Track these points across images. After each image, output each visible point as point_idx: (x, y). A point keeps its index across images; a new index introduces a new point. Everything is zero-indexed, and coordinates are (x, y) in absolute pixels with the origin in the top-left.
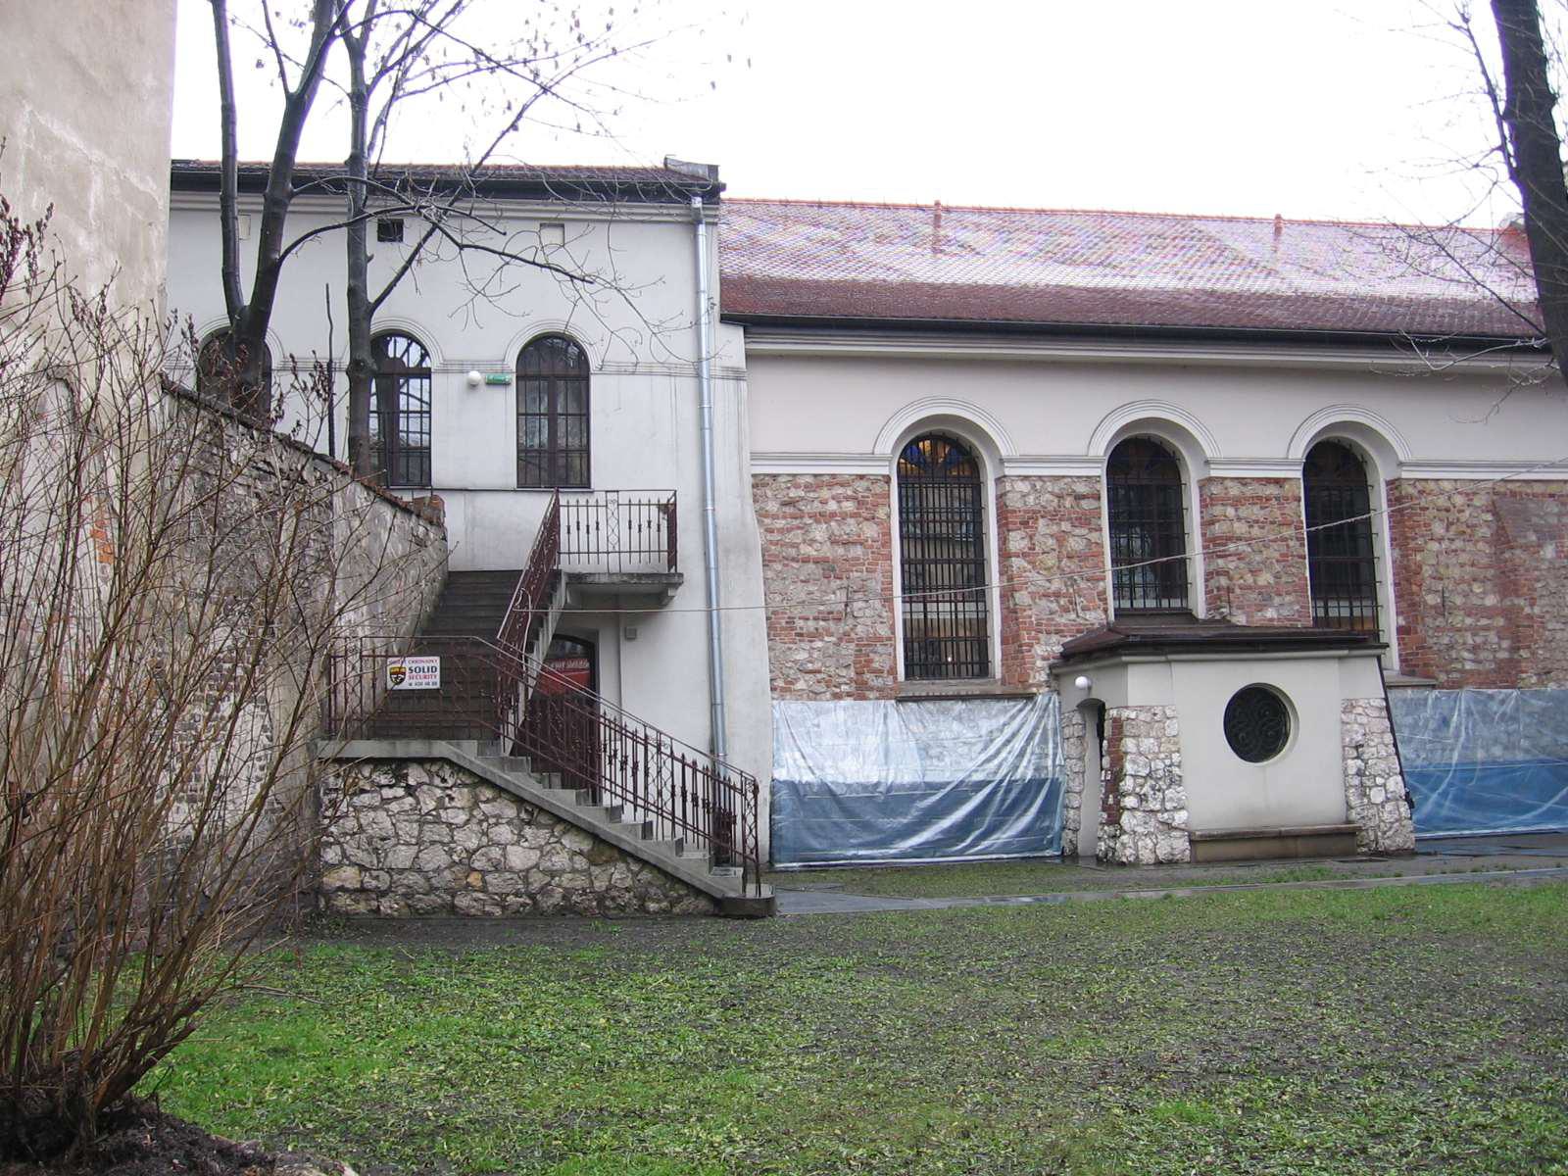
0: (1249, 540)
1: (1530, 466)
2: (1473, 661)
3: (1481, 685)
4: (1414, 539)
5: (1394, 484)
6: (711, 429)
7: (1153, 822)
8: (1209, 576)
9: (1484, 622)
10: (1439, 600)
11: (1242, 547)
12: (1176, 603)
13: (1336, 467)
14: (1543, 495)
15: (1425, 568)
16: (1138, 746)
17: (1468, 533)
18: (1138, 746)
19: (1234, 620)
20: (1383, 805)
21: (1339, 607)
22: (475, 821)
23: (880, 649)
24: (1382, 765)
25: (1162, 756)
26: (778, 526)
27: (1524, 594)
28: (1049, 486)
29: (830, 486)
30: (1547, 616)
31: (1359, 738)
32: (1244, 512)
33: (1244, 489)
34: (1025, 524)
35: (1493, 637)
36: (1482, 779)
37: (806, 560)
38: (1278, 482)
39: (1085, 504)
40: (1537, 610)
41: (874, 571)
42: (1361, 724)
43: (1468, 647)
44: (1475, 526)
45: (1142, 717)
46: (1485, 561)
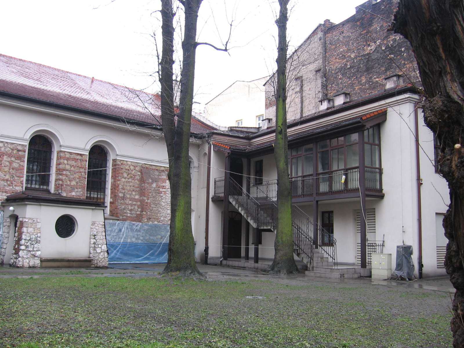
0: (70, 171)
1: (152, 161)
2: (130, 214)
3: (132, 221)
4: (118, 177)
5: (114, 160)
7: (29, 254)
8: (56, 180)
9: (134, 203)
10: (123, 195)
11: (68, 173)
12: (45, 187)
13: (99, 153)
14: (155, 169)
15: (120, 186)
16: (27, 230)
17: (133, 177)
18: (27, 230)
19: (62, 194)
20: (100, 253)
21: (94, 194)
24: (101, 241)
25: (35, 234)
27: (146, 196)
28: (9, 146)
30: (152, 203)
31: (95, 233)
32: (70, 162)
33: (70, 155)
36: (129, 247)
38: (81, 155)
39: (20, 153)
40: (149, 201)
42: (96, 229)
44: (135, 175)
45: (30, 221)
46: (137, 186)
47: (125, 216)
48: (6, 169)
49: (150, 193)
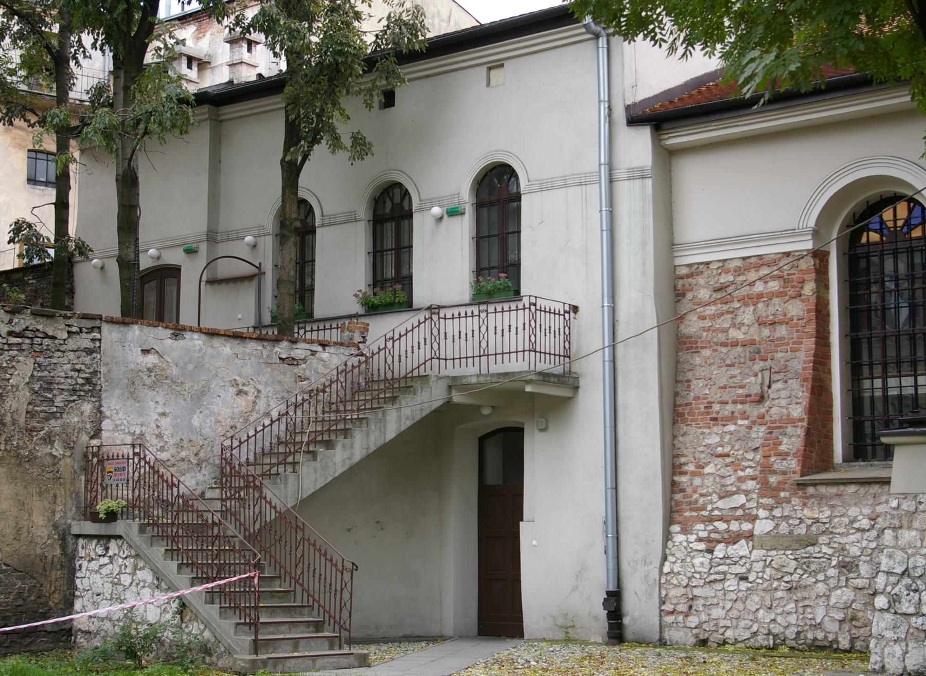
6: (602, 231)
7: (904, 628)
16: (896, 538)
18: (896, 538)
22: (134, 584)
23: (789, 430)
26: (708, 312)
29: (758, 267)
37: (735, 344)
41: (799, 350)
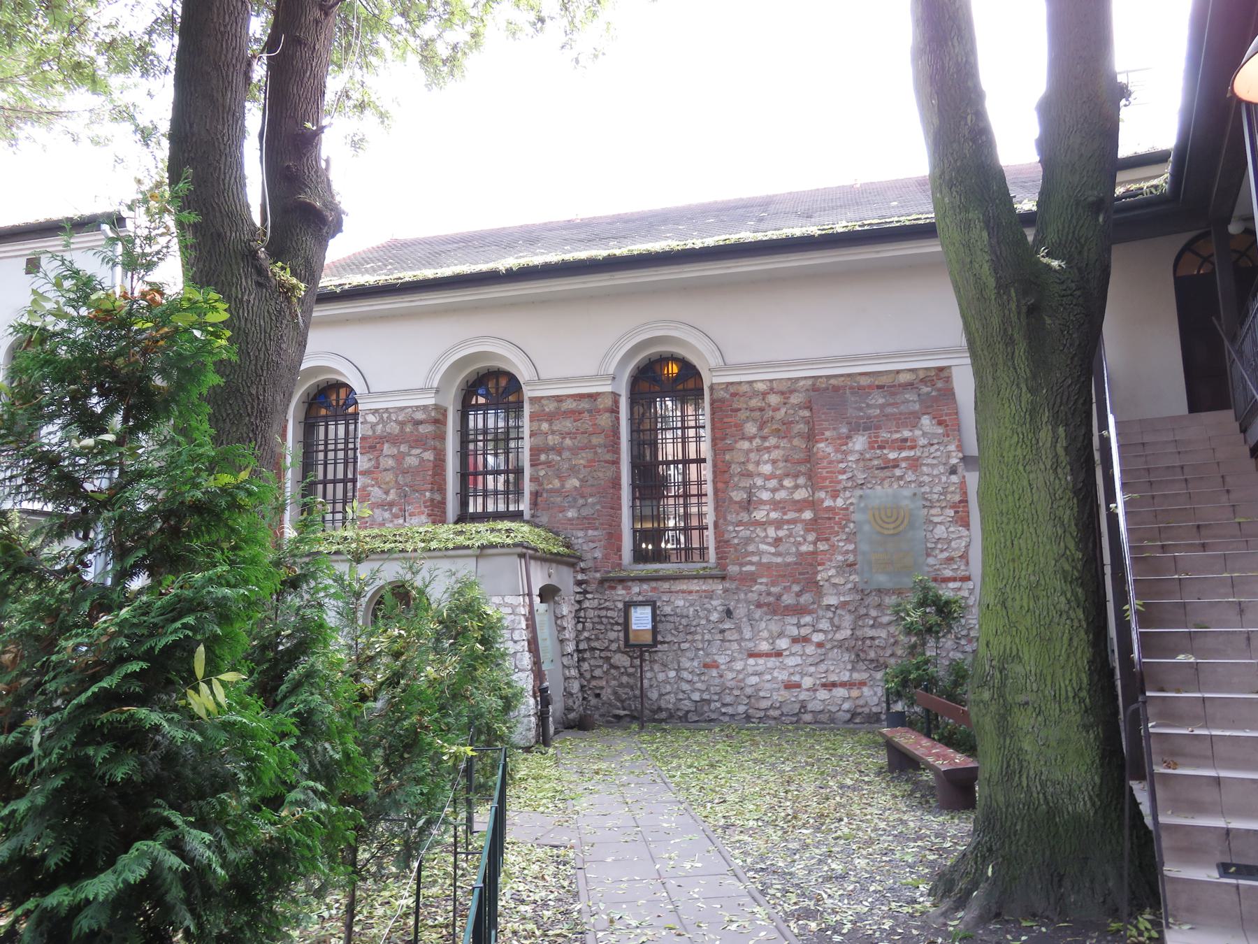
1: (855, 358)
4: (724, 439)
9: (791, 515)
14: (870, 387)
34: (373, 448)
35: (799, 529)
39: (422, 429)
40: (840, 502)
43: (770, 540)
44: (792, 422)
47: (751, 563)
48: (389, 477)
49: (843, 472)
